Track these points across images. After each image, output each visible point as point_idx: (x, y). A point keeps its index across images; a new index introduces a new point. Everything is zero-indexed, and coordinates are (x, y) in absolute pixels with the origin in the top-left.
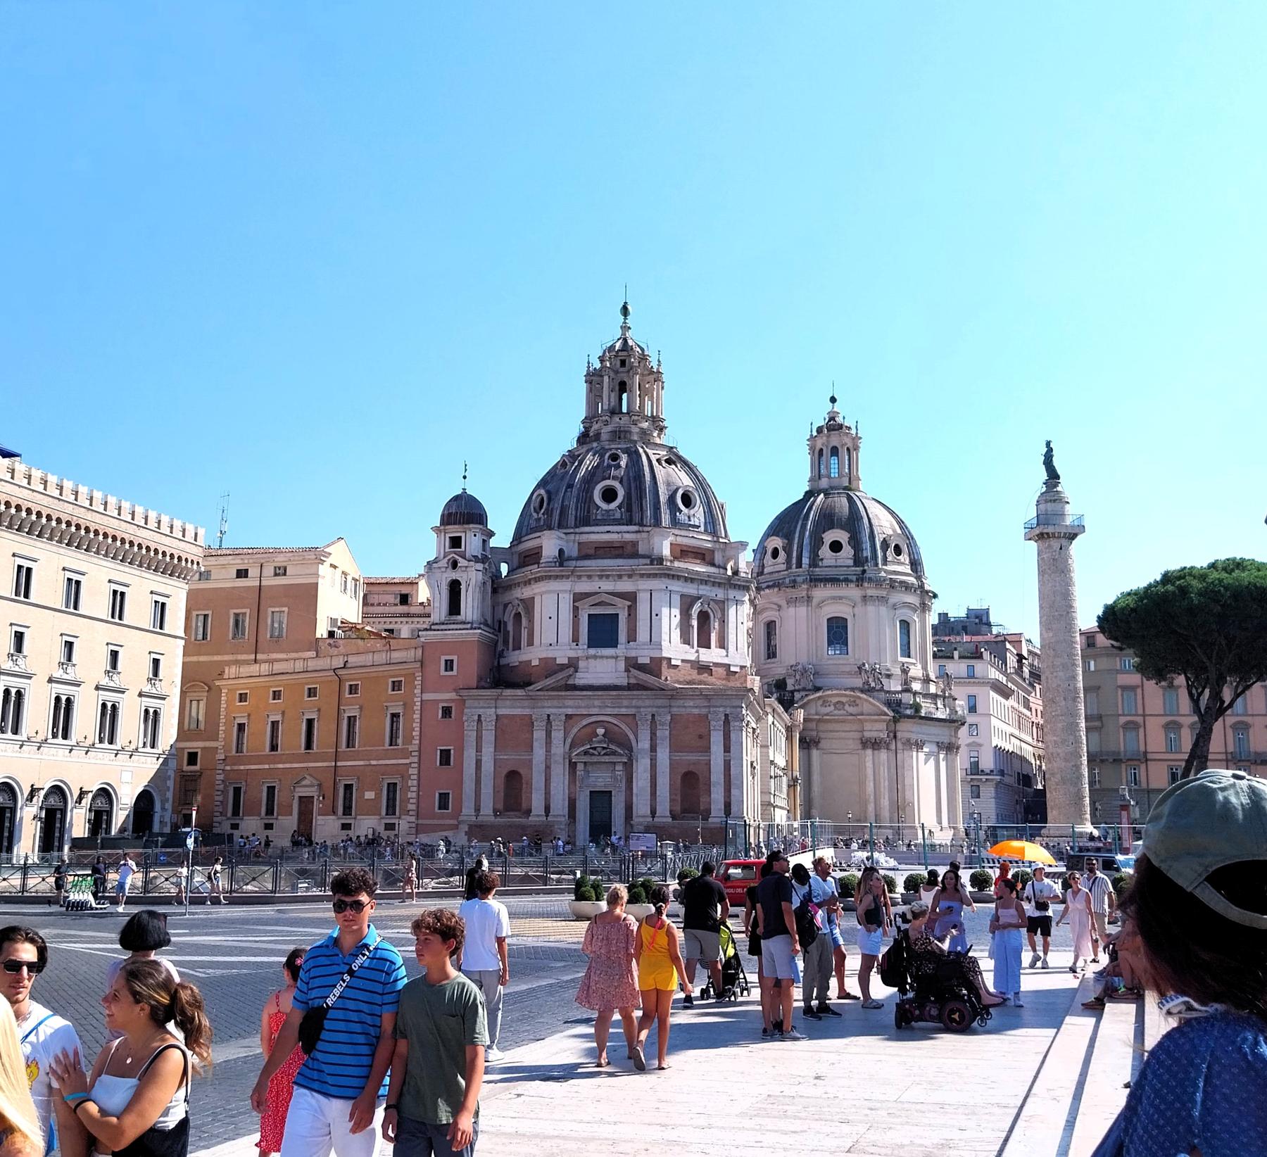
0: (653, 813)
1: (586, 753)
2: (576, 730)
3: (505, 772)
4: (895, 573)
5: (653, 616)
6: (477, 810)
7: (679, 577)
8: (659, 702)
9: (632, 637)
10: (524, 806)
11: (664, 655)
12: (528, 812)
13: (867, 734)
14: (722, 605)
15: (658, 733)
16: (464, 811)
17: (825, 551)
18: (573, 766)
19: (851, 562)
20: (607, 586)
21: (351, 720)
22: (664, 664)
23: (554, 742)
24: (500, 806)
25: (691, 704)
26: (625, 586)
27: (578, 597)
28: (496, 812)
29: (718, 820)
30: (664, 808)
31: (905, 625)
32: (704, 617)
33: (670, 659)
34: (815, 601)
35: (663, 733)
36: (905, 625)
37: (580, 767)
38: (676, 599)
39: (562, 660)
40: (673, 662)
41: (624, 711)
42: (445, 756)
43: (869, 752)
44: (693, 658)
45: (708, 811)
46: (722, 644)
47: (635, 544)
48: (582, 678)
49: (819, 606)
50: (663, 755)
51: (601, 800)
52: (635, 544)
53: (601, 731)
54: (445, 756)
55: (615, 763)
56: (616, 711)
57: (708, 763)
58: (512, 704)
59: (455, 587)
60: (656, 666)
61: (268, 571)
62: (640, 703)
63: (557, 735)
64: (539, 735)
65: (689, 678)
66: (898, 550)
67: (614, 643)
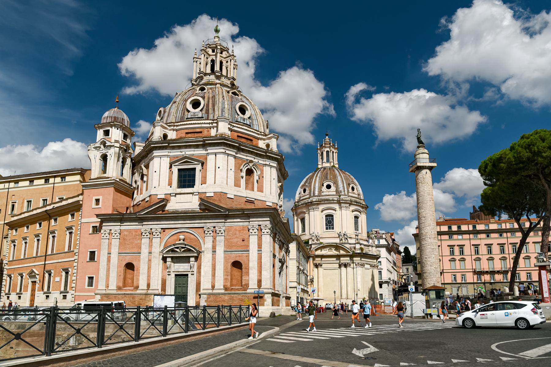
0: (213, 287)
1: (172, 251)
2: (168, 237)
3: (125, 263)
4: (352, 197)
9: (204, 182)
10: (135, 284)
12: (137, 288)
15: (218, 238)
16: (99, 288)
18: (164, 259)
19: (335, 193)
23: (154, 245)
24: (121, 284)
28: (119, 288)
29: (253, 291)
30: (220, 284)
31: (356, 217)
32: (250, 172)
36: (356, 217)
37: (169, 260)
38: (232, 160)
40: (229, 196)
41: (196, 225)
45: (247, 285)
46: (261, 190)
53: (182, 237)
55: (189, 257)
56: (192, 226)
57: (248, 256)
63: (156, 241)
66: (353, 189)
67: (192, 186)
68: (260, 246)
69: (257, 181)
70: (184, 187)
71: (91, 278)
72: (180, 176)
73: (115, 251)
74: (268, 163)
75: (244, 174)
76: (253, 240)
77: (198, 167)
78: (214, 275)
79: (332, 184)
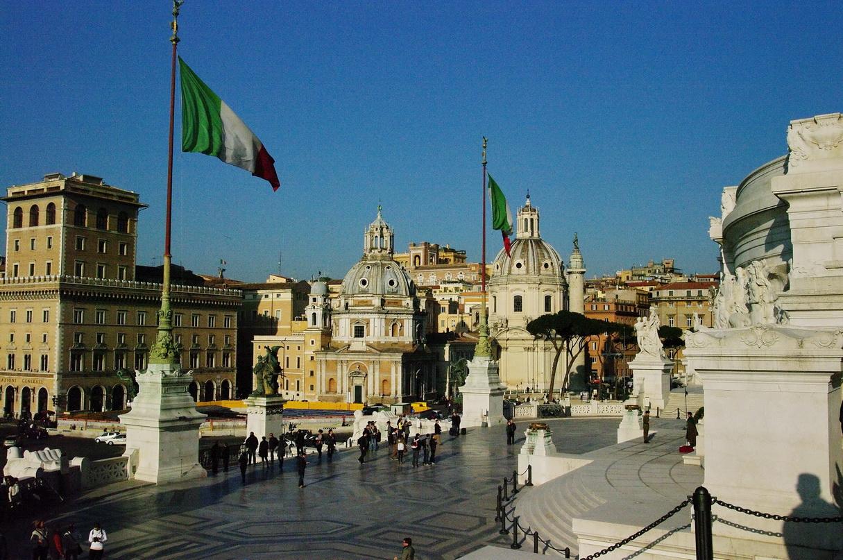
6: (321, 391)
8: (376, 357)
9: (368, 335)
12: (336, 392)
13: (525, 346)
17: (514, 267)
18: (350, 377)
19: (525, 272)
20: (360, 316)
21: (288, 358)
25: (385, 357)
27: (352, 321)
28: (327, 392)
30: (377, 392)
34: (510, 289)
35: (377, 367)
37: (352, 378)
38: (383, 321)
42: (312, 373)
43: (526, 352)
47: (371, 301)
49: (512, 291)
50: (377, 374)
51: (358, 389)
52: (371, 301)
54: (312, 373)
58: (331, 357)
59: (314, 315)
61: (275, 295)
62: (371, 357)
63: (345, 367)
64: (339, 367)
66: (546, 266)
68: (396, 373)
70: (358, 337)
71: (312, 387)
72: (356, 330)
73: (324, 371)
75: (390, 328)
76: (393, 369)
78: (374, 387)
79: (522, 263)
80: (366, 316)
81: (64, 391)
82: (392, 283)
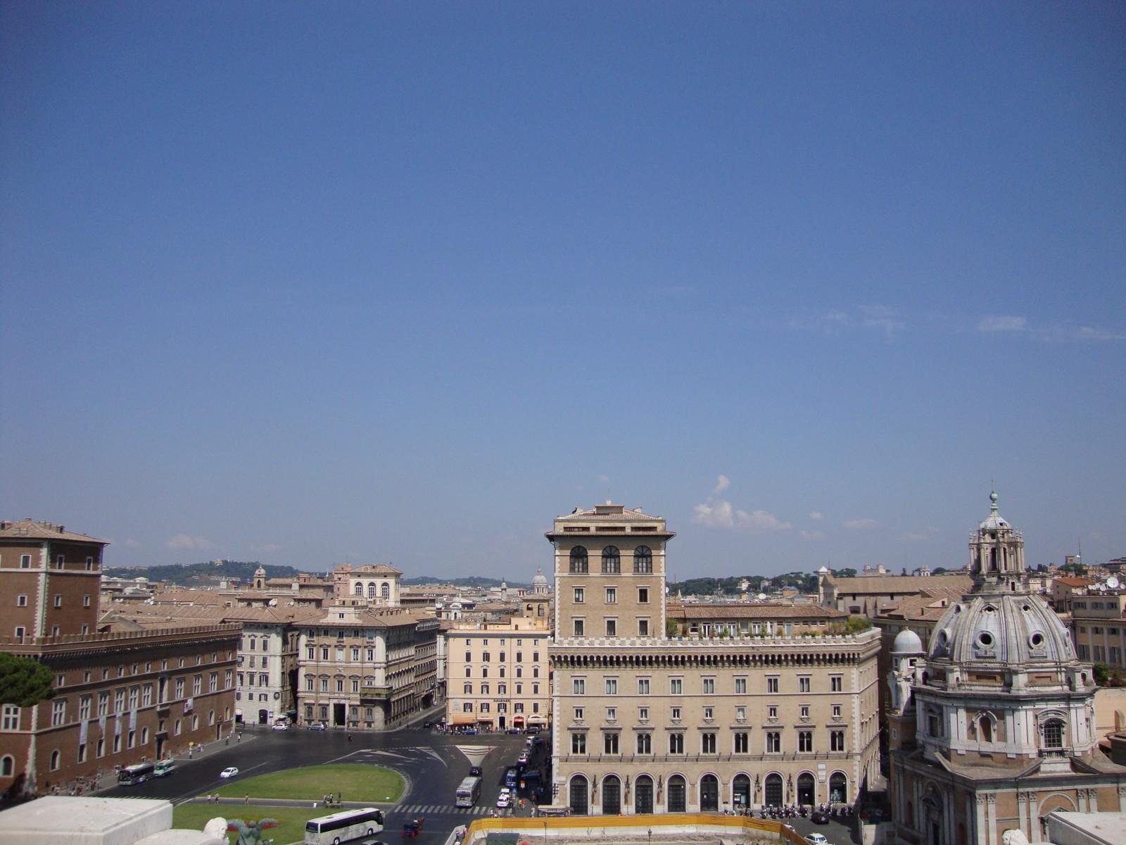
5: (949, 722)
7: (961, 699)
11: (952, 747)
12: (913, 828)
14: (1002, 717)
22: (953, 752)
26: (939, 701)
27: (927, 704)
33: (957, 750)
39: (921, 742)
40: (959, 752)
44: (977, 750)
46: (1003, 737)
48: (927, 756)
51: (936, 828)
60: (947, 755)
65: (974, 762)
69: (994, 730)
74: (1008, 707)
77: (938, 719)
80: (939, 701)
81: (563, 779)
82: (986, 639)
